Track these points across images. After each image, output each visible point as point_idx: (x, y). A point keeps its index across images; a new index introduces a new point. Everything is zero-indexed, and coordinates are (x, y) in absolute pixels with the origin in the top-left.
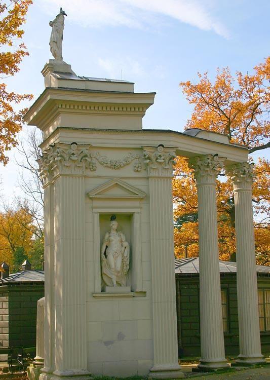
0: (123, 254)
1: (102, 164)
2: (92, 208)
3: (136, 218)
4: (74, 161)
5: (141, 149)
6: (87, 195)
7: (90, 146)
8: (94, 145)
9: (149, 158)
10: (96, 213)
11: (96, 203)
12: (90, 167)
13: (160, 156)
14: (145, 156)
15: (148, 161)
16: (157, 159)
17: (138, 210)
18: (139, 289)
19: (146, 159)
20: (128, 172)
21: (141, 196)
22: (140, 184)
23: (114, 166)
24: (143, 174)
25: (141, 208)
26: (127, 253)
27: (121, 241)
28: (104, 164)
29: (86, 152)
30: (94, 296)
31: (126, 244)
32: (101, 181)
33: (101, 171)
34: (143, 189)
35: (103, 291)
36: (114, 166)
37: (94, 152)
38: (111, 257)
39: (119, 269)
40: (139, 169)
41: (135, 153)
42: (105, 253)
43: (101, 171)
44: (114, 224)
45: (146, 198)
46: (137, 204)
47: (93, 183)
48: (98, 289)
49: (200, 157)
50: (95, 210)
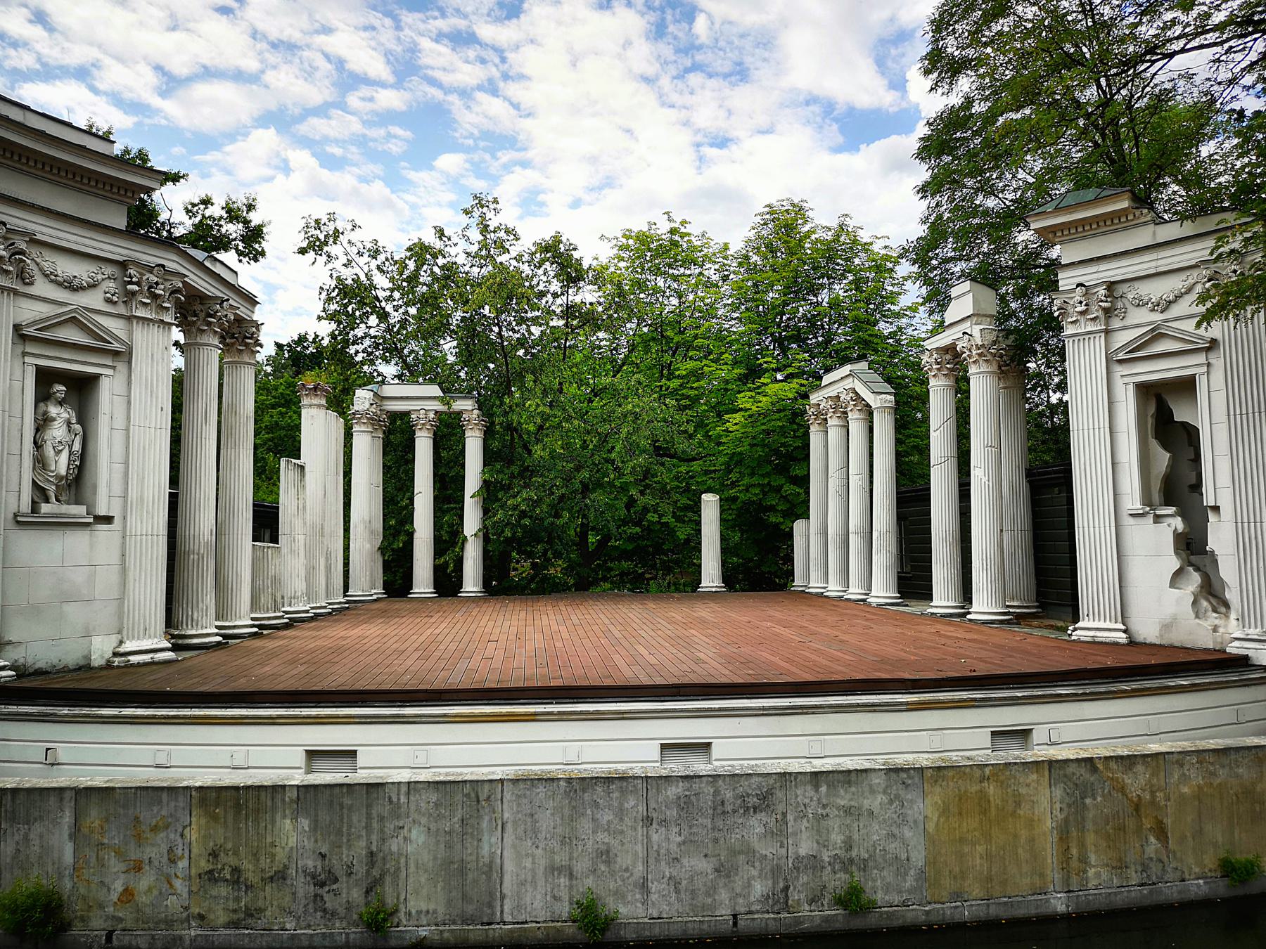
0: (71, 447)
1: (47, 276)
2: (24, 354)
3: (104, 384)
5: (123, 265)
6: (17, 328)
7: (33, 241)
8: (39, 237)
9: (137, 284)
10: (31, 365)
12: (23, 276)
13: (157, 284)
14: (130, 277)
15: (135, 288)
16: (151, 287)
17: (110, 372)
18: (102, 512)
19: (131, 283)
20: (93, 300)
21: (117, 346)
22: (115, 326)
23: (71, 286)
25: (114, 368)
26: (77, 446)
27: (69, 423)
29: (23, 246)
30: (20, 522)
32: (44, 310)
33: (41, 287)
34: (121, 334)
36: (71, 286)
37: (34, 251)
38: (49, 452)
39: (63, 471)
40: (115, 299)
41: (109, 270)
42: (35, 443)
43: (41, 287)
44: (60, 389)
45: (123, 355)
47: (29, 312)
48: (26, 506)
49: (202, 298)
50: (27, 359)
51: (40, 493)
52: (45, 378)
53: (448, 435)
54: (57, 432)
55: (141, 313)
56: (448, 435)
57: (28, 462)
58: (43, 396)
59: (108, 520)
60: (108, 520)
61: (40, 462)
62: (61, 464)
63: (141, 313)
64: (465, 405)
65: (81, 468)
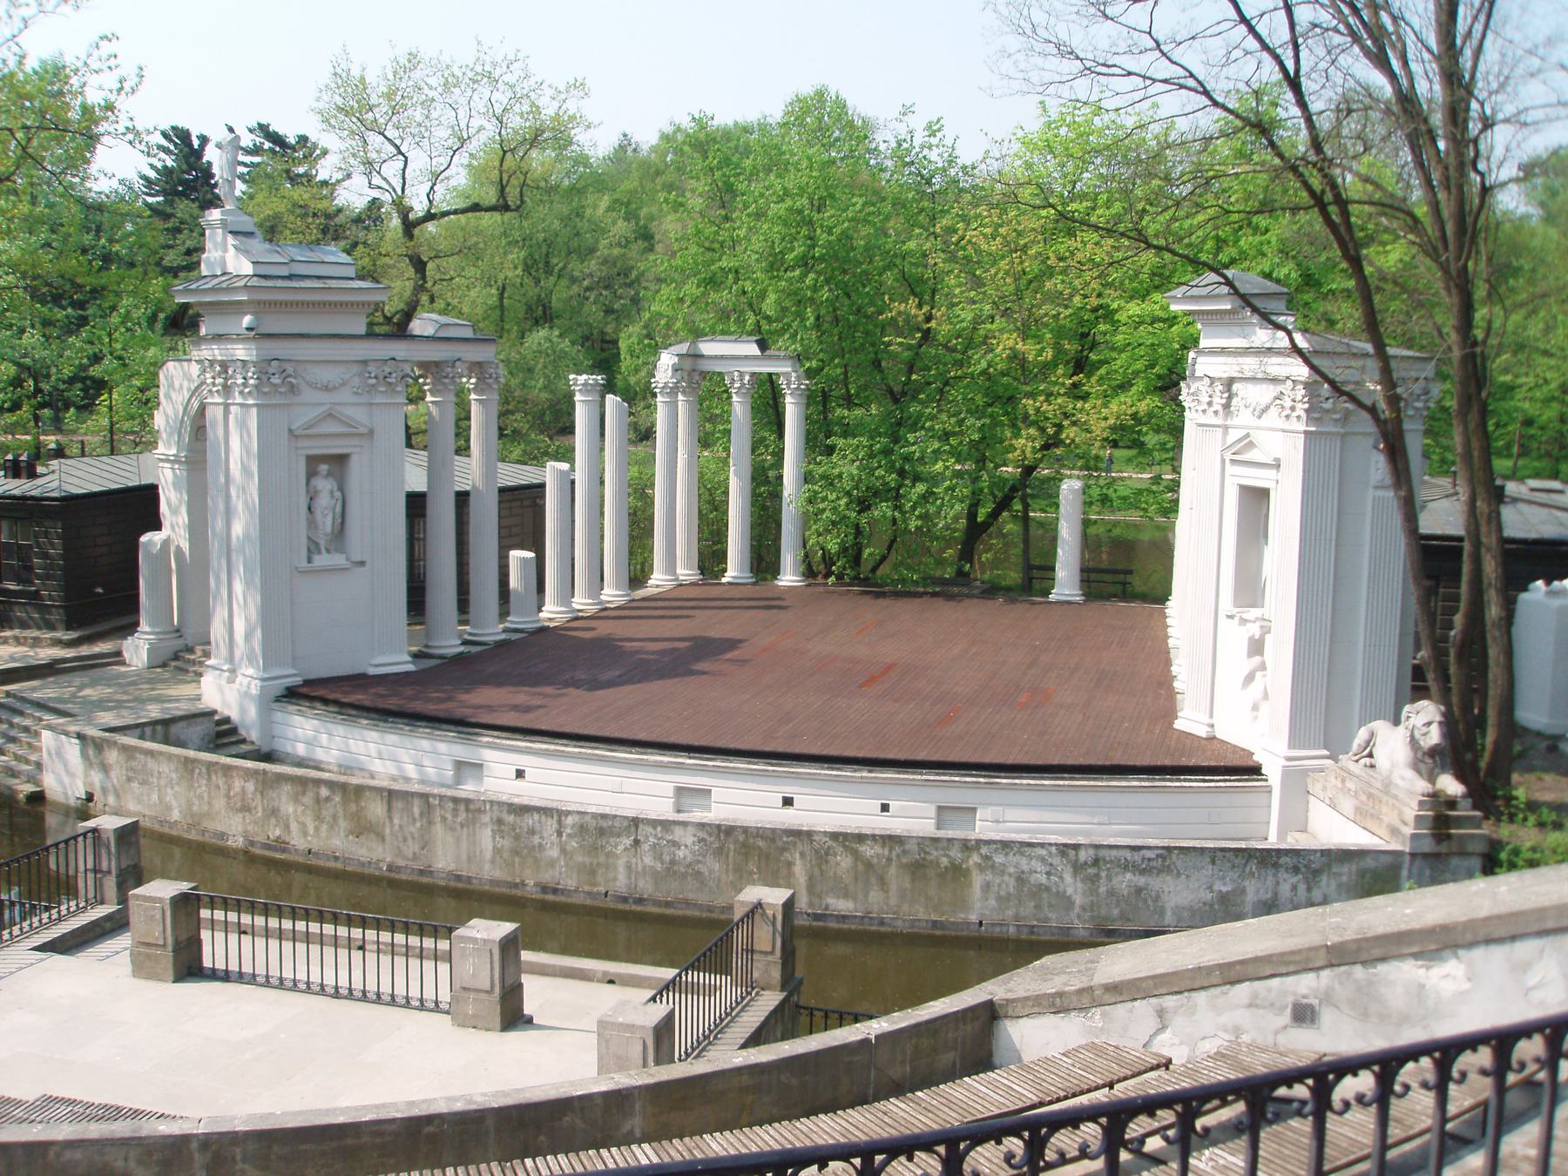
4: (275, 385)
5: (365, 362)
6: (290, 431)
11: (301, 443)
12: (293, 389)
15: (373, 381)
20: (345, 396)
21: (362, 430)
22: (359, 414)
23: (326, 388)
24: (365, 399)
26: (338, 509)
27: (332, 492)
28: (313, 385)
31: (338, 494)
33: (309, 395)
35: (309, 561)
36: (326, 388)
39: (329, 529)
41: (356, 369)
43: (309, 395)
44: (324, 468)
46: (356, 442)
51: (313, 549)
52: (313, 462)
53: (768, 400)
54: (324, 501)
55: (379, 399)
56: (768, 400)
57: (303, 523)
58: (311, 474)
59: (362, 563)
60: (362, 563)
61: (312, 524)
62: (327, 523)
63: (379, 399)
64: (784, 370)
65: (343, 523)
